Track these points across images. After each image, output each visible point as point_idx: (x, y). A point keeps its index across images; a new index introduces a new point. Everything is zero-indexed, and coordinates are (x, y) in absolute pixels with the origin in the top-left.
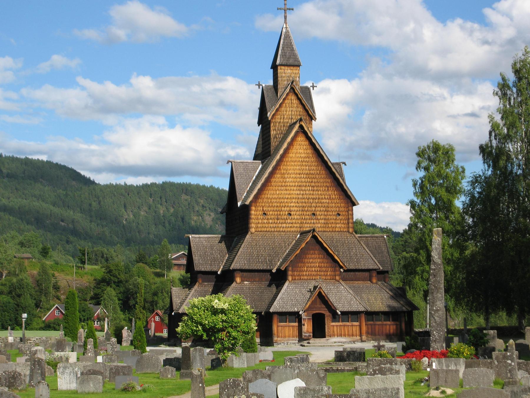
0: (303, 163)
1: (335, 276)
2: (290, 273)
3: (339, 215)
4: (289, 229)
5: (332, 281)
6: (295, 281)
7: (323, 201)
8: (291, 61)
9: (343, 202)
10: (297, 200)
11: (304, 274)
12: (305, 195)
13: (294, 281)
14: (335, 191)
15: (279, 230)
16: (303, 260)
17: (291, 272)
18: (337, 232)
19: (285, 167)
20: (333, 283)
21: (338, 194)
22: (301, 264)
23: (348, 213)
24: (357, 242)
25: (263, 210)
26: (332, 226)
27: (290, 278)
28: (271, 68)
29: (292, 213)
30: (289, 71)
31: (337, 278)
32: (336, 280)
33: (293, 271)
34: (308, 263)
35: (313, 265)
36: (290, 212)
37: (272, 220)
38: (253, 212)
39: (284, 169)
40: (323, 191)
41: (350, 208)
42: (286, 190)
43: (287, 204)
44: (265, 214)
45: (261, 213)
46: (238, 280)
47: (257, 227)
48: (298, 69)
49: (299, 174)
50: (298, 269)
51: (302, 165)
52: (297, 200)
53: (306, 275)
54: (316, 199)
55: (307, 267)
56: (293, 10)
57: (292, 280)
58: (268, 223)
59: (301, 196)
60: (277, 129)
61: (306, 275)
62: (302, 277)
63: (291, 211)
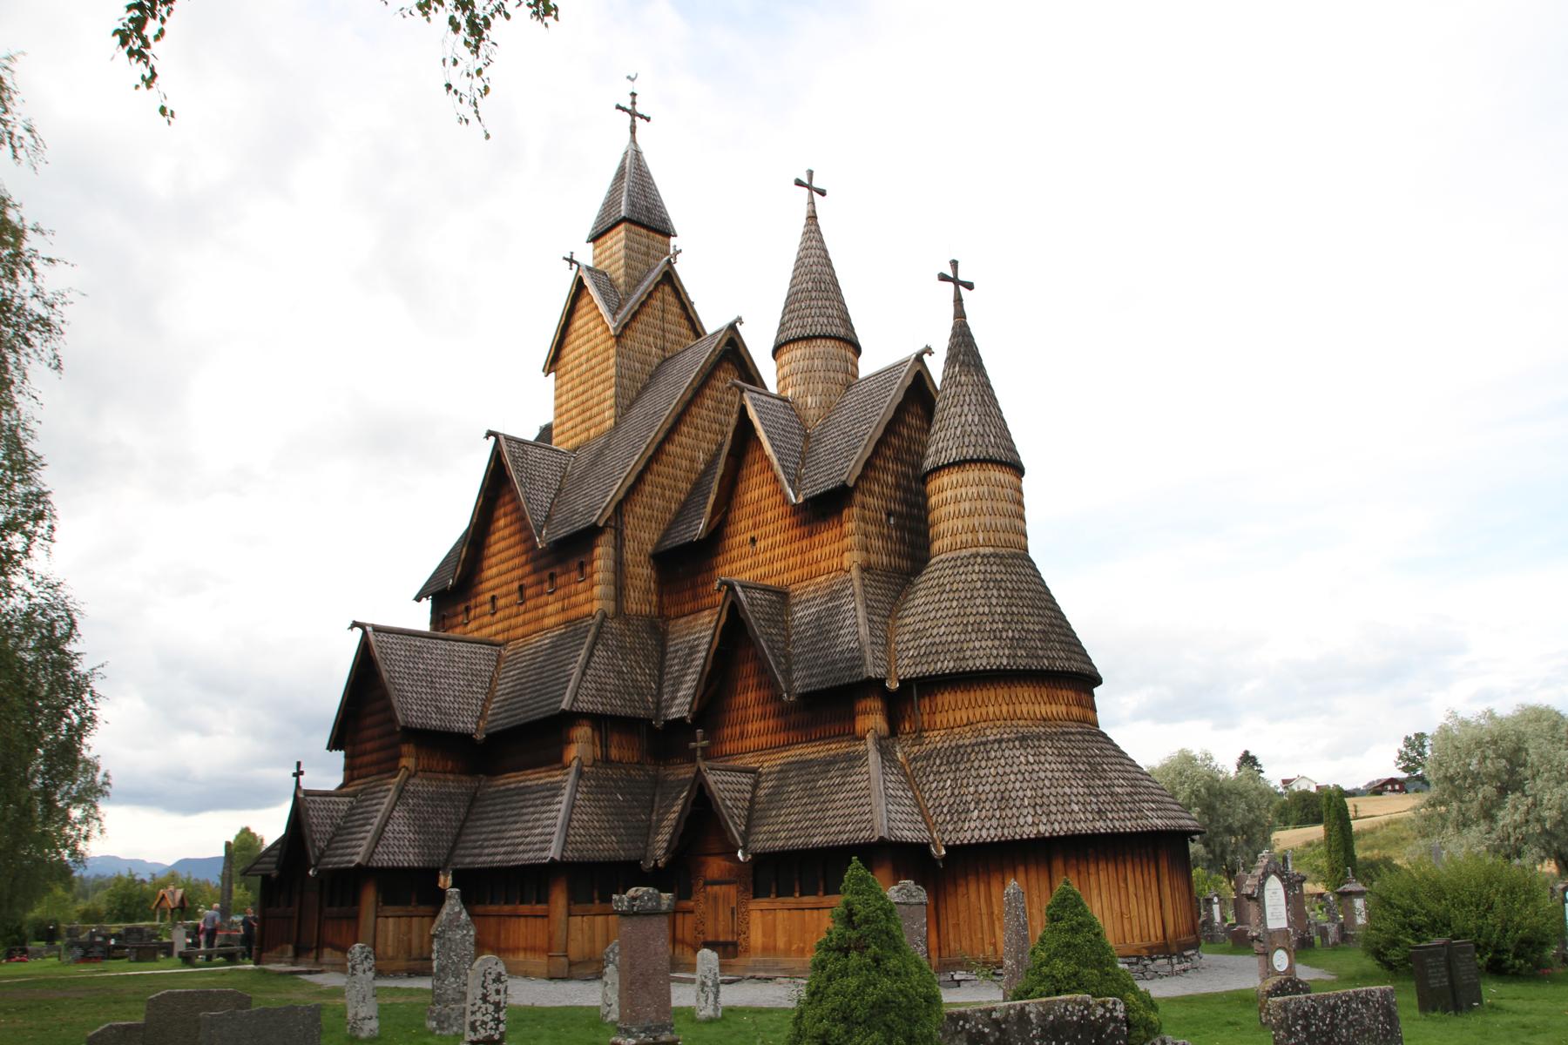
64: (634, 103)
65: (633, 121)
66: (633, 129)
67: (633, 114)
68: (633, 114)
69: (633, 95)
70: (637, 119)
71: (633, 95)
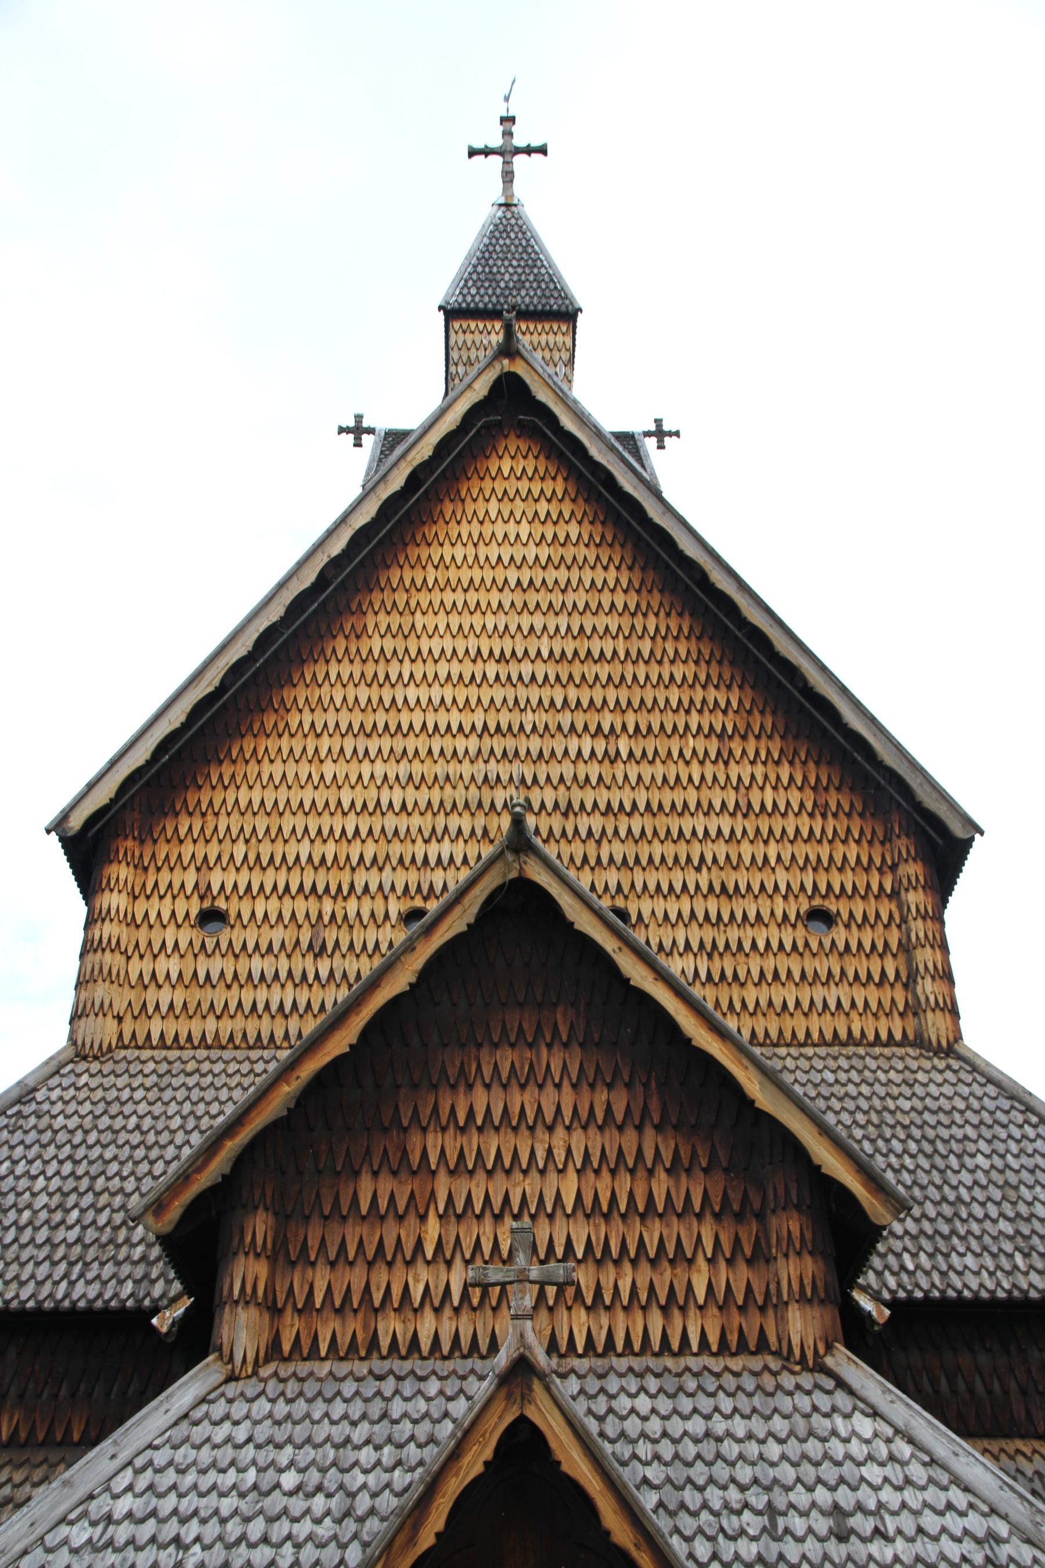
3: (821, 916)
5: (736, 1364)
6: (303, 1368)
9: (849, 831)
11: (417, 1293)
17: (260, 1269)
18: (823, 1042)
19: (395, 620)
22: (386, 1185)
24: (1006, 1104)
25: (204, 892)
32: (784, 1355)
49: (502, 659)
50: (353, 1234)
57: (273, 1351)
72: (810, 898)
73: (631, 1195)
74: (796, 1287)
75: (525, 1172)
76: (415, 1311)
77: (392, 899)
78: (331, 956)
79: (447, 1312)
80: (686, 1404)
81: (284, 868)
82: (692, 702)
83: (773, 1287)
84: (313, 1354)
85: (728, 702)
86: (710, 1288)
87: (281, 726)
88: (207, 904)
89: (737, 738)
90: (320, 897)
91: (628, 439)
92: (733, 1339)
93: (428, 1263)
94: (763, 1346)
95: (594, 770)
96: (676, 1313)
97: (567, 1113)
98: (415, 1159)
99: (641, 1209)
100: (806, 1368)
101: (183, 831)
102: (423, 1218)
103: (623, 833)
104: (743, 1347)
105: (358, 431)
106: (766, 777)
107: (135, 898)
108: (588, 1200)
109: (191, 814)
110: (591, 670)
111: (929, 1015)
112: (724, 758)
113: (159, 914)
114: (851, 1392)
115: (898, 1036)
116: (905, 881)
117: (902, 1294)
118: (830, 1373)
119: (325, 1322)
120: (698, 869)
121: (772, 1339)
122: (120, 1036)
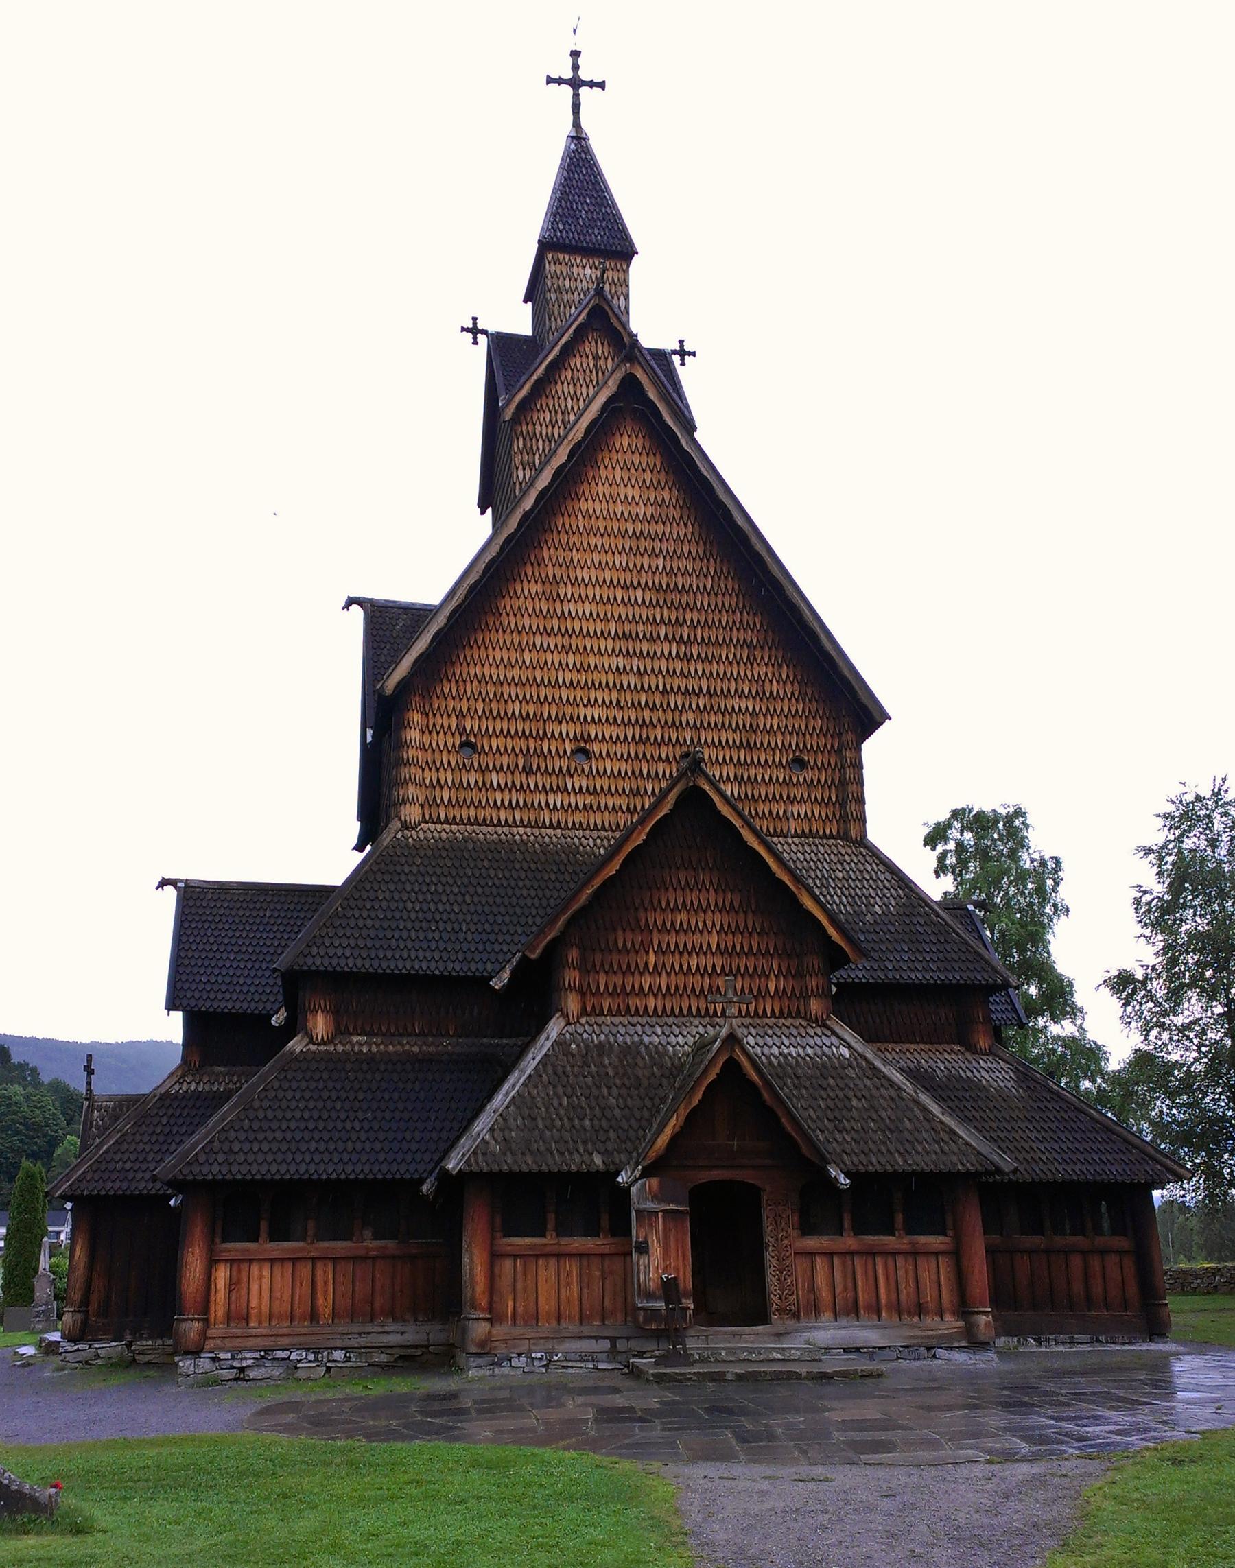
0: (643, 544)
1: (806, 998)
2: (571, 976)
3: (800, 763)
4: (579, 817)
5: (788, 1022)
6: (600, 1020)
7: (736, 703)
8: (596, 237)
10: (615, 695)
11: (646, 987)
12: (653, 677)
13: (593, 1020)
14: (780, 666)
15: (533, 818)
16: (642, 914)
18: (796, 835)
20: (795, 1032)
21: (795, 676)
22: (629, 936)
23: (842, 758)
24: (889, 876)
25: (461, 731)
26: (770, 812)
27: (572, 1004)
28: (525, 301)
29: (596, 748)
30: (588, 271)
31: (815, 1006)
33: (586, 968)
34: (663, 930)
35: (691, 939)
36: (582, 745)
37: (502, 774)
38: (413, 735)
39: (557, 563)
40: (731, 663)
41: (849, 737)
42: (567, 650)
43: (569, 710)
44: (466, 744)
45: (453, 741)
46: (320, 1025)
47: (434, 804)
48: (625, 267)
49: (625, 587)
50: (615, 958)
51: (637, 552)
52: (615, 695)
53: (655, 992)
54: (698, 695)
55: (660, 952)
56: (603, 89)
57: (583, 1012)
58: (485, 787)
59: (633, 680)
60: (537, 461)
61: (655, 992)
62: (635, 1002)
63: (588, 740)
64: (575, 67)
65: (576, 96)
66: (576, 107)
67: (576, 83)
68: (576, 83)
69: (575, 54)
70: (584, 91)
71: (575, 54)
72: (794, 752)
73: (742, 944)
74: (815, 989)
75: (693, 932)
76: (645, 995)
77: (567, 742)
78: (536, 774)
79: (660, 996)
80: (769, 1041)
81: (506, 719)
82: (734, 622)
83: (804, 989)
84: (602, 1014)
85: (755, 623)
86: (776, 988)
87: (498, 624)
88: (464, 738)
89: (758, 648)
90: (527, 738)
91: (661, 357)
92: (786, 1011)
93: (650, 973)
94: (798, 1015)
95: (678, 665)
96: (761, 1000)
97: (713, 904)
98: (643, 923)
99: (746, 951)
100: (818, 1025)
101: (446, 691)
102: (647, 953)
103: (694, 707)
104: (790, 1015)
105: (474, 331)
106: (774, 675)
107: (423, 733)
108: (722, 946)
109: (450, 681)
110: (676, 597)
111: (852, 822)
112: (751, 661)
113: (438, 744)
114: (838, 1037)
115: (834, 833)
116: (845, 743)
117: (842, 981)
118: (829, 1028)
119: (605, 999)
120: (734, 731)
121: (803, 1011)
122: (424, 815)
